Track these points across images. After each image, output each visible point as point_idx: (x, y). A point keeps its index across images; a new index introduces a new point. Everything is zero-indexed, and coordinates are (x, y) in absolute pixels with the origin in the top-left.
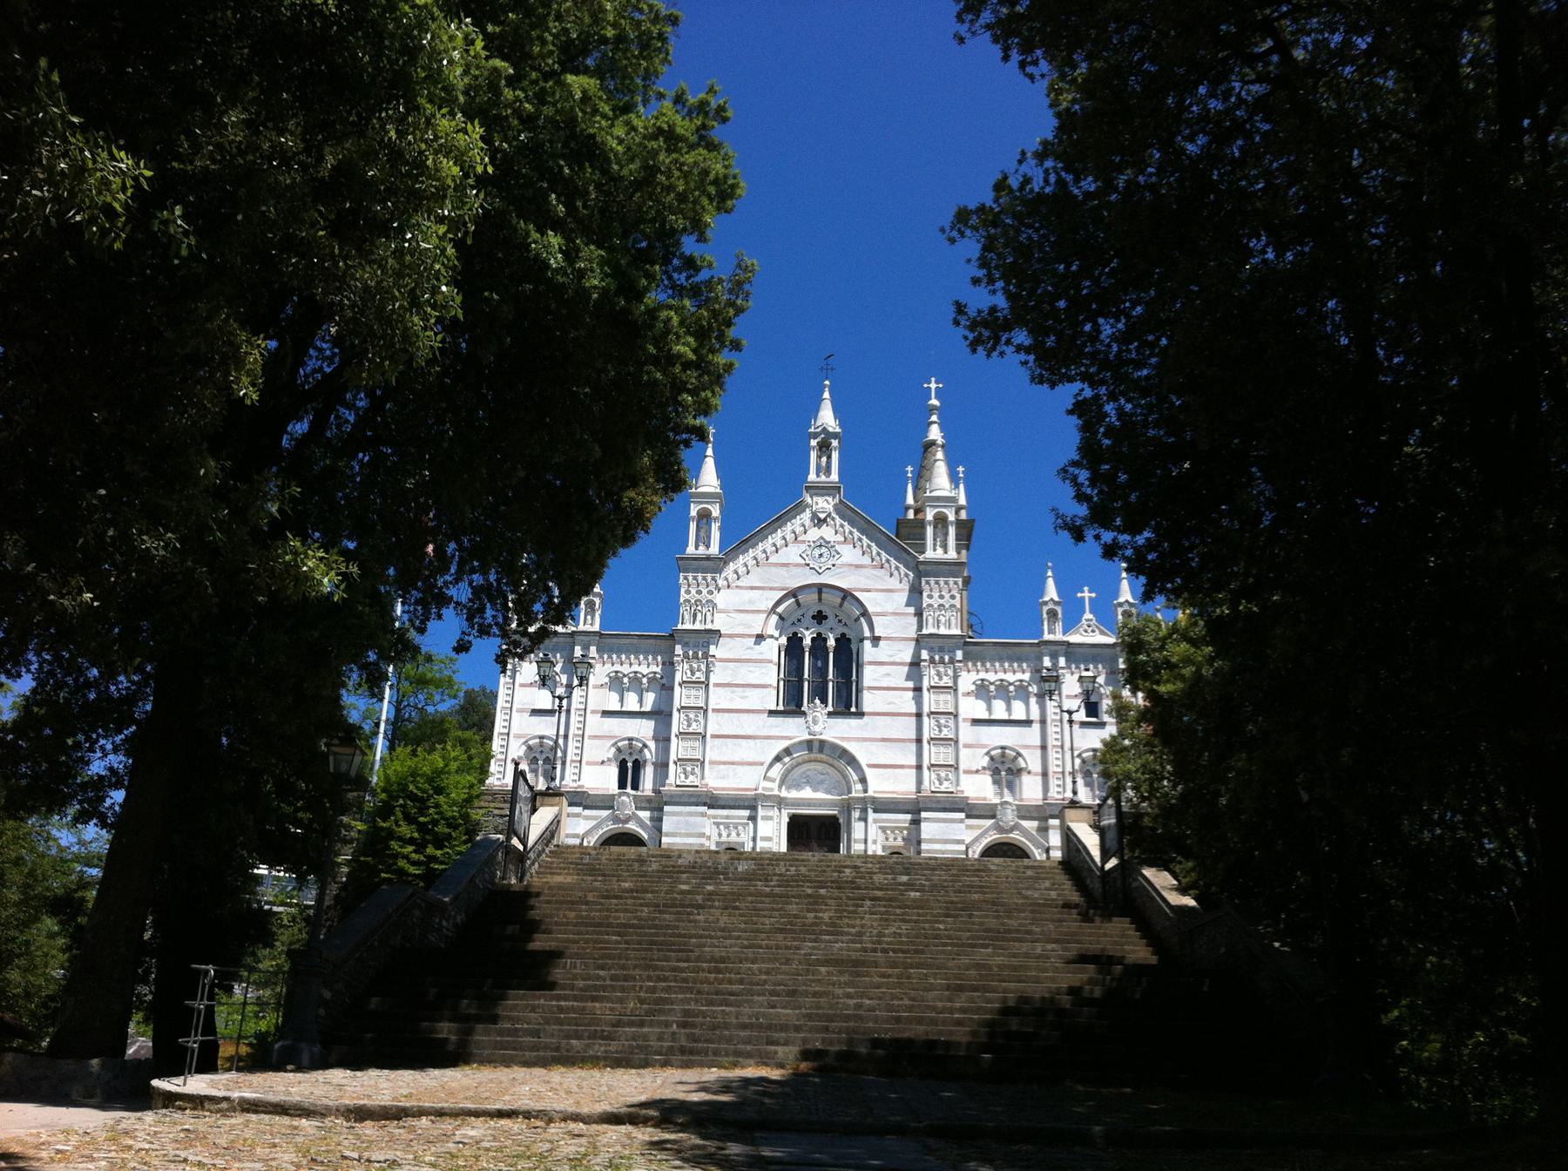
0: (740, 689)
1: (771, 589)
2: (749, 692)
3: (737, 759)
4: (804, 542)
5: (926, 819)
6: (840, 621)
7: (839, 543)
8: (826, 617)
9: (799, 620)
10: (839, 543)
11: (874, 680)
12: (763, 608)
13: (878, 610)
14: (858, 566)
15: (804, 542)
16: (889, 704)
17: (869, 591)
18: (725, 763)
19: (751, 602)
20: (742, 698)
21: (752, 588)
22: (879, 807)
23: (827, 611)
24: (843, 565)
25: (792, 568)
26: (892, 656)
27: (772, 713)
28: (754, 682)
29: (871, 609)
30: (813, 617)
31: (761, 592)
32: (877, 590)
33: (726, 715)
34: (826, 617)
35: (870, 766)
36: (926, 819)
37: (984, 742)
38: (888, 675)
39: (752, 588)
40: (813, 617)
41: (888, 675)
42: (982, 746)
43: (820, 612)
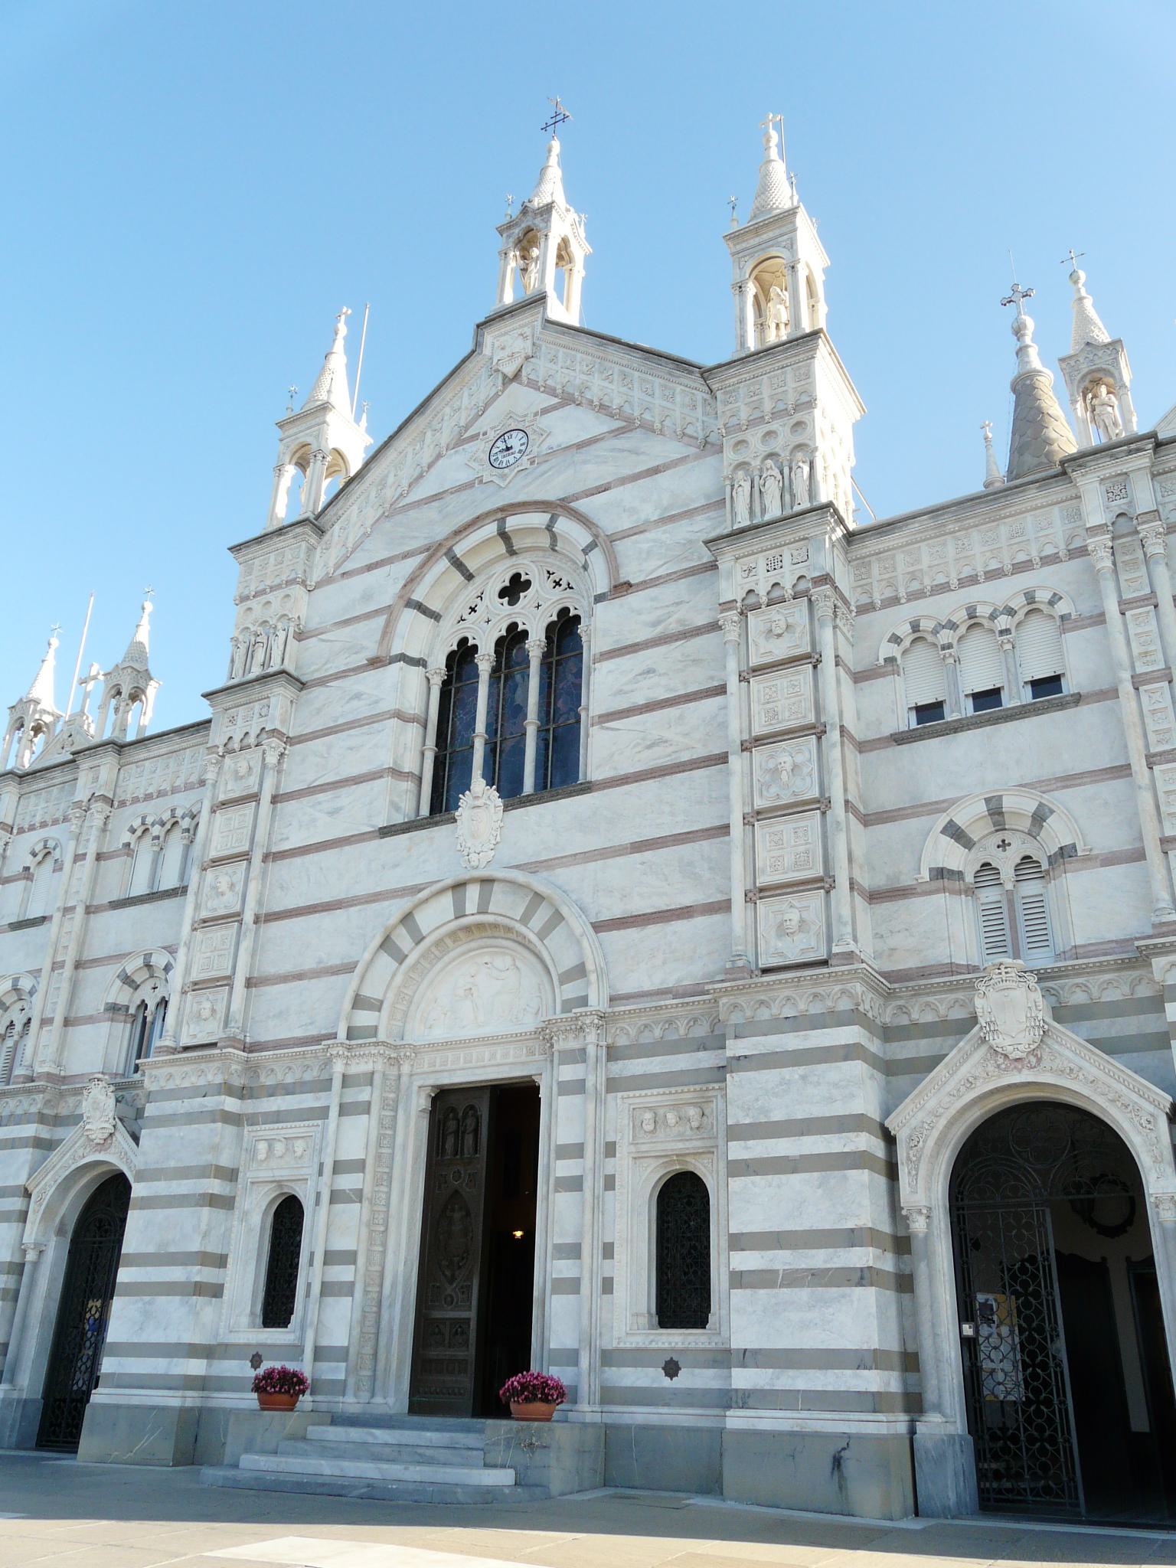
0: (329, 794)
1: (406, 556)
2: (347, 797)
3: (309, 964)
4: (474, 437)
5: (741, 1062)
6: (558, 583)
7: (545, 411)
8: (527, 584)
9: (473, 610)
10: (545, 411)
11: (620, 692)
12: (386, 598)
13: (626, 524)
14: (580, 446)
15: (474, 437)
16: (649, 747)
17: (605, 488)
18: (285, 978)
19: (367, 597)
20: (334, 812)
21: (370, 568)
22: (622, 1041)
23: (529, 567)
24: (553, 453)
25: (449, 498)
26: (655, 624)
27: (386, 832)
28: (354, 772)
29: (610, 523)
30: (503, 594)
31: (386, 568)
32: (623, 481)
33: (298, 860)
34: (527, 584)
35: (599, 927)
36: (741, 1062)
37: (933, 794)
38: (650, 671)
39: (370, 568)
40: (503, 594)
41: (650, 671)
42: (936, 808)
43: (516, 578)
